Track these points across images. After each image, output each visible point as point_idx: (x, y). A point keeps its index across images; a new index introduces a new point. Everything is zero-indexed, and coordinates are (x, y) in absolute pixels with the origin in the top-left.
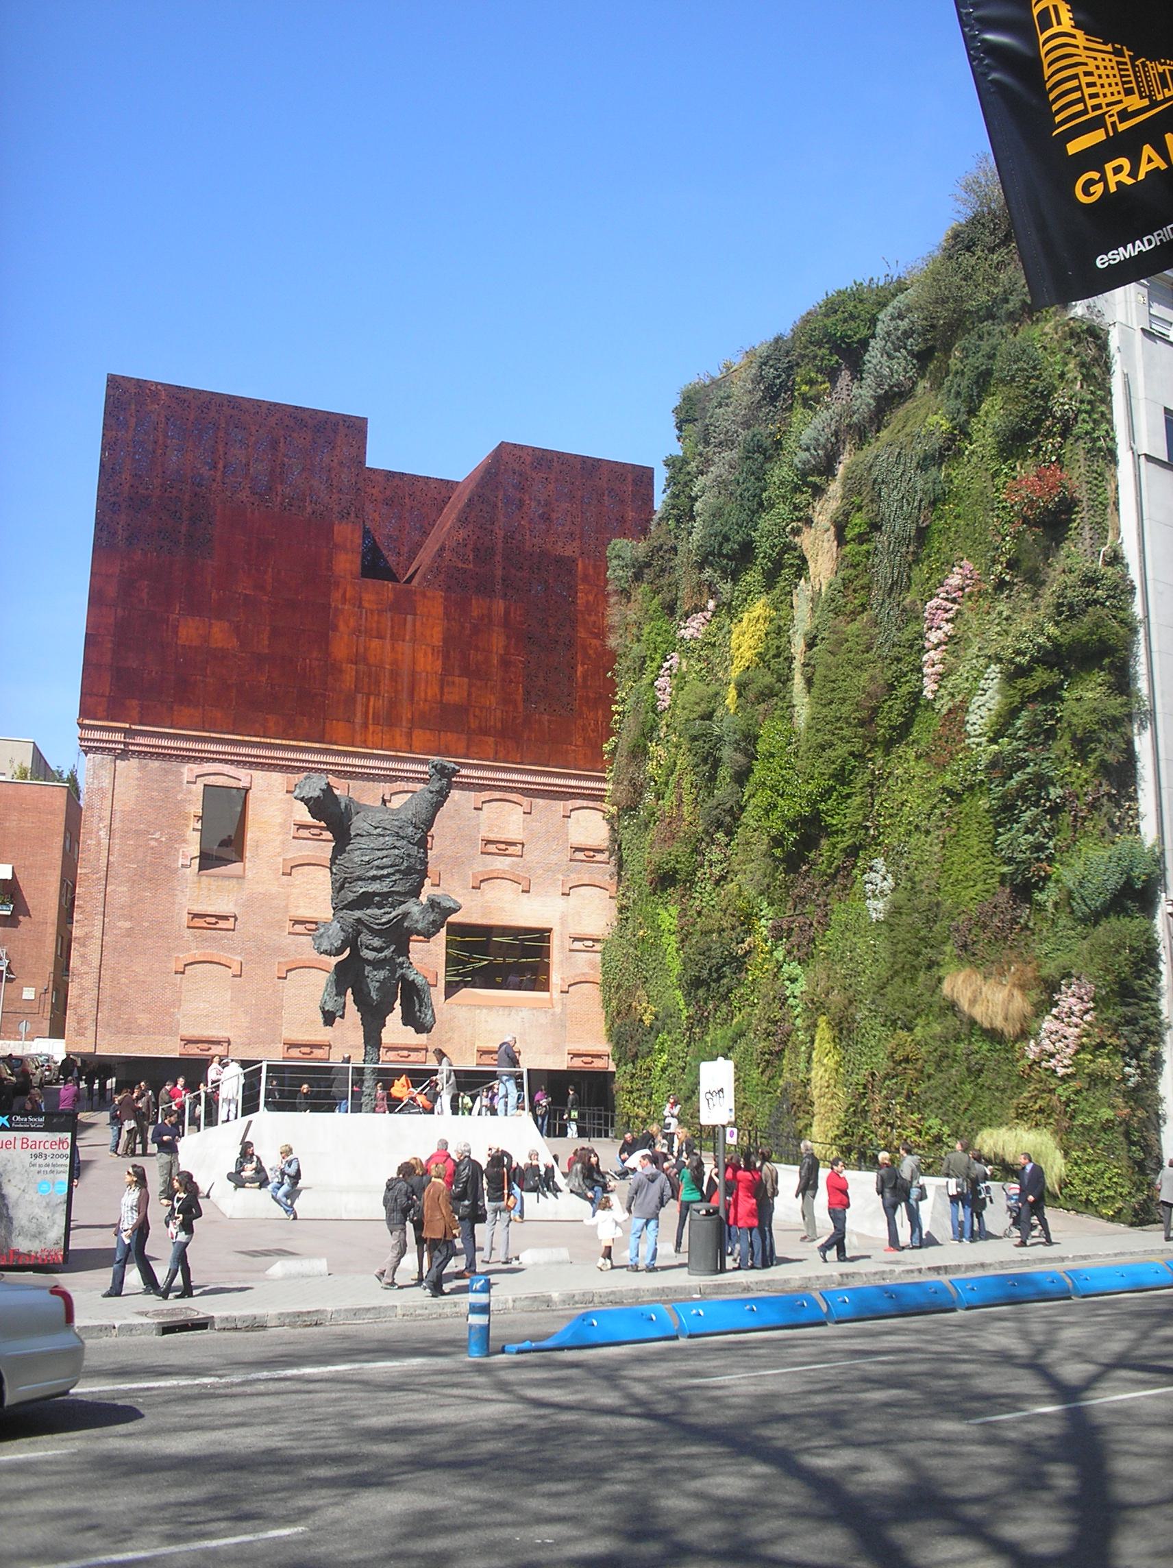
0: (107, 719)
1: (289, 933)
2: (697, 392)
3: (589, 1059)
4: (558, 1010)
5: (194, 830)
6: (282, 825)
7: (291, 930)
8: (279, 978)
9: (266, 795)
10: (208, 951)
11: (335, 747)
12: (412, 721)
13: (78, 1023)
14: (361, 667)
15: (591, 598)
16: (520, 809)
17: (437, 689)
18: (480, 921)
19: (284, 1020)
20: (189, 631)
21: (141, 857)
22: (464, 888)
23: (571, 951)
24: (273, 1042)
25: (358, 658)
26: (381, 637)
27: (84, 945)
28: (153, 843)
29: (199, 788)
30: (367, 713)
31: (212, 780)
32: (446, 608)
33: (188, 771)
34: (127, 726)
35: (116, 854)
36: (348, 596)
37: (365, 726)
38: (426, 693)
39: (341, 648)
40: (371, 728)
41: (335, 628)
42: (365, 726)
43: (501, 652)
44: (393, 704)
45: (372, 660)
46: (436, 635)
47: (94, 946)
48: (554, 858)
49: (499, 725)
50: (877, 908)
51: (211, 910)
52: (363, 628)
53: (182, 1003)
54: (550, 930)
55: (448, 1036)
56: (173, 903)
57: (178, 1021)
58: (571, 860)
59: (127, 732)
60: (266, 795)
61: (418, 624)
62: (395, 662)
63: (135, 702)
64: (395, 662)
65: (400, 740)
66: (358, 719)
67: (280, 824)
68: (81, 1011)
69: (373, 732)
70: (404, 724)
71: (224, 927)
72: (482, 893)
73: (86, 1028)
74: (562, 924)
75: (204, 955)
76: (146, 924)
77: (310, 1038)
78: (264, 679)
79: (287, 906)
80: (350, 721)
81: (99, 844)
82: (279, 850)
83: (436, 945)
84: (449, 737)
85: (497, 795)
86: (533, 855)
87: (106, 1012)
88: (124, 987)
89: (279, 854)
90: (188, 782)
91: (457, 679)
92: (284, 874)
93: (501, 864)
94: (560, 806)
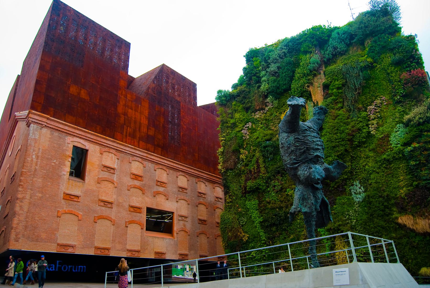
0: (41, 112)
1: (99, 205)
2: (259, 51)
3: (183, 256)
4: (176, 239)
5: (69, 161)
6: (98, 165)
7: (99, 204)
10: (70, 209)
11: (117, 141)
12: (139, 138)
13: (16, 236)
14: (126, 117)
15: (184, 114)
16: (166, 173)
17: (146, 129)
18: (155, 208)
20: (73, 90)
21: (48, 169)
23: (179, 220)
24: (91, 247)
25: (125, 114)
26: (132, 109)
27: (22, 202)
28: (53, 164)
29: (71, 146)
30: (127, 133)
32: (149, 105)
33: (69, 139)
34: (49, 117)
35: (38, 166)
37: (126, 136)
38: (143, 129)
39: (120, 109)
40: (128, 137)
41: (119, 103)
42: (126, 136)
43: (163, 123)
45: (129, 116)
46: (146, 113)
47: (26, 201)
48: (174, 190)
49: (162, 145)
50: (358, 198)
51: (73, 193)
53: (59, 230)
54: (173, 213)
55: (147, 247)
56: (59, 189)
57: (57, 237)
58: (179, 191)
59: (48, 119)
61: (142, 108)
62: (135, 118)
63: (52, 109)
64: (135, 118)
65: (136, 143)
66: (124, 134)
67: (98, 165)
68: (18, 231)
70: (137, 138)
71: (76, 200)
72: (156, 198)
73: (19, 238)
74: (177, 211)
75: (69, 211)
76: (48, 196)
77: (104, 246)
78: (97, 113)
79: (98, 195)
80: (122, 133)
81: (32, 160)
83: (143, 215)
84: (149, 146)
85: (161, 167)
87: (28, 232)
88: (37, 221)
89: (97, 176)
90: (68, 143)
91: (152, 128)
92: (98, 183)
93: (161, 189)
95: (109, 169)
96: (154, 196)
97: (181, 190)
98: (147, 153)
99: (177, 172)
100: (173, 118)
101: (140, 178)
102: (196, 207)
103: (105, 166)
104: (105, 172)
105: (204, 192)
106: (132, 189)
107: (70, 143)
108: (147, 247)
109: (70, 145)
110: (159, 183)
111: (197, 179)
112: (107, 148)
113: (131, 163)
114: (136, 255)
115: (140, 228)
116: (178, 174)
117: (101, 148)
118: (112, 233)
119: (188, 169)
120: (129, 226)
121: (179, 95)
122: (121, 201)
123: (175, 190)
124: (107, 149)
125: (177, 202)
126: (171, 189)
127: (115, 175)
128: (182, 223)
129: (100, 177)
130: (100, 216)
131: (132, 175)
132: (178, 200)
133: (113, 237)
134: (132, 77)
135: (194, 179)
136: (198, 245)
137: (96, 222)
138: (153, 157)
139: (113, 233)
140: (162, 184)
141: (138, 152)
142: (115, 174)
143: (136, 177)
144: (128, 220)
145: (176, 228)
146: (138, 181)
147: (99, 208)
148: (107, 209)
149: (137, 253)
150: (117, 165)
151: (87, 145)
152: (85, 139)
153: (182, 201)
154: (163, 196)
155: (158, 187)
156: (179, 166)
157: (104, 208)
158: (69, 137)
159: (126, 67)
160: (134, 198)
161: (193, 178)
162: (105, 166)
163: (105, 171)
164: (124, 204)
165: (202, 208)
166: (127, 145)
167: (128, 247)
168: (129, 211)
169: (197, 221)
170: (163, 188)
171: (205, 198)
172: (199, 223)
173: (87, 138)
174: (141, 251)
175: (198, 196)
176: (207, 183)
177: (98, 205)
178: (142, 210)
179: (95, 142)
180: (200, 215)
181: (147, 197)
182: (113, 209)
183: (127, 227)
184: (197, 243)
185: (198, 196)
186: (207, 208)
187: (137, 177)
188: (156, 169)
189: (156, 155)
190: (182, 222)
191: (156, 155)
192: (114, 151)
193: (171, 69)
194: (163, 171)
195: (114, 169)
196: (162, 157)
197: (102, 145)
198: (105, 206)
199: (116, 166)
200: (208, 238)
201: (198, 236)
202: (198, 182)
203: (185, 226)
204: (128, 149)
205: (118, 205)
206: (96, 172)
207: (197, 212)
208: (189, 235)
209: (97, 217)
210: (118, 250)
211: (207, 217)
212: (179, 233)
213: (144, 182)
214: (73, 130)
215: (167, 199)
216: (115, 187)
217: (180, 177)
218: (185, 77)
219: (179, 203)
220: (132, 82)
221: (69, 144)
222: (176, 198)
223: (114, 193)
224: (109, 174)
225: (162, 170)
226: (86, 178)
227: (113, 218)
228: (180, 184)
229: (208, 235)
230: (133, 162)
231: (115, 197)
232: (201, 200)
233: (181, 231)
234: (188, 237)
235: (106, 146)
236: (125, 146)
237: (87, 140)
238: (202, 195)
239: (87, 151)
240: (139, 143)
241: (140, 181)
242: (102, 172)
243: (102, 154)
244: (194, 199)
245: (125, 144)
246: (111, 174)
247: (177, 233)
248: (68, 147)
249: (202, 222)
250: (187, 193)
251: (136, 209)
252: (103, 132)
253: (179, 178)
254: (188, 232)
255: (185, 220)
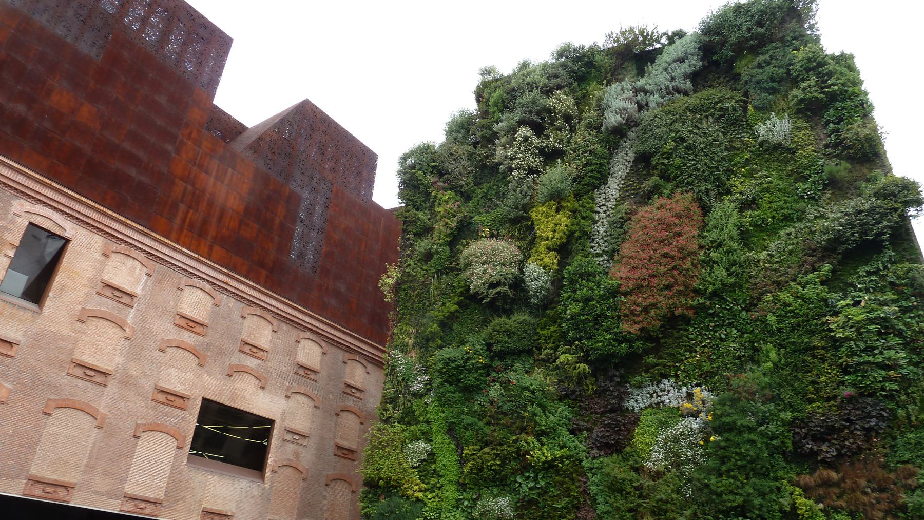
1: (68, 374)
5: (6, 255)
6: (89, 280)
7: (70, 371)
8: (46, 414)
9: (84, 251)
14: (190, 187)
16: (270, 327)
18: (227, 403)
19: (37, 456)
22: (221, 374)
23: (284, 440)
24: (18, 476)
29: (23, 223)
31: (38, 221)
33: (20, 206)
36: (193, 136)
40: (185, 231)
44: (205, 222)
48: (286, 369)
52: (197, 162)
54: (271, 422)
55: (182, 495)
58: (296, 373)
60: (84, 251)
66: (178, 220)
67: (89, 278)
69: (186, 235)
70: (209, 238)
79: (72, 350)
82: (81, 299)
83: (191, 414)
85: (259, 311)
86: (273, 363)
90: (15, 214)
92: (79, 320)
93: (251, 363)
94: (294, 333)
95: (118, 294)
96: (230, 376)
97: (301, 372)
98: (228, 275)
99: (299, 332)
100: (310, 214)
101: (198, 329)
102: (335, 417)
103: (108, 286)
104: (106, 299)
105: (359, 386)
106: (170, 350)
107: (23, 214)
108: (182, 495)
109: (19, 220)
110: (247, 349)
111: (347, 355)
112: (123, 245)
113: (181, 290)
114: (147, 511)
115: (174, 444)
116: (302, 334)
117: (109, 241)
118: (89, 448)
119: (328, 329)
120: (144, 436)
121: (333, 170)
122: (134, 374)
123: (288, 369)
124: (123, 247)
125: (288, 397)
126: (277, 364)
127: (133, 311)
128: (291, 447)
129: (89, 307)
130: (64, 400)
131: (178, 317)
132: (289, 394)
133: (90, 457)
134: (242, 124)
135: (341, 355)
136: (325, 507)
137: (49, 415)
138: (242, 287)
139: (94, 446)
140: (254, 350)
141: (204, 269)
142: (132, 307)
143: (190, 323)
144: (143, 422)
145: (271, 459)
146: (192, 334)
147: (66, 380)
148: (90, 385)
149: (152, 506)
150: (143, 289)
151: (69, 229)
152: (66, 213)
153: (300, 398)
154: (253, 378)
155: (243, 356)
156: (307, 319)
157: (80, 383)
158: (22, 201)
159: (213, 83)
160: (173, 371)
161: (338, 351)
162: (108, 286)
163: (106, 297)
164: (143, 381)
165: (350, 420)
166: (178, 247)
167: (129, 489)
168: (152, 400)
169: (331, 450)
170: (257, 362)
171: (361, 399)
172: (335, 455)
173: (74, 214)
174: (165, 503)
175: (344, 392)
176: (369, 366)
177: (64, 374)
178: (191, 402)
179: (93, 226)
180: (342, 437)
181: (210, 374)
182: (108, 389)
183: (138, 438)
184: (324, 502)
185: (344, 392)
186: (361, 423)
187: (191, 324)
188: (246, 315)
189: (251, 283)
190: (291, 445)
191: (225, 270)
192: (141, 257)
193: (322, 112)
194: (263, 322)
195: (131, 295)
196: (265, 290)
197: (112, 235)
198: (88, 378)
199: (138, 291)
200: (353, 492)
201: (327, 485)
202: (349, 362)
203: (297, 455)
204: (181, 257)
205: (126, 381)
206: (81, 293)
207: (335, 428)
208: (305, 480)
209: (55, 400)
210: (95, 493)
211: (358, 442)
212: (280, 471)
213: (206, 340)
214: (38, 188)
215: (263, 388)
216: (126, 338)
217: (303, 342)
218: (353, 137)
219: (292, 402)
220: (240, 133)
221: (19, 216)
222: (286, 387)
223: (119, 351)
224: (115, 304)
225: (263, 320)
226: (48, 303)
227: (102, 409)
228: (302, 358)
229: (354, 486)
230: (187, 289)
231: (119, 360)
232: (350, 403)
233: (285, 468)
234: (302, 484)
235: (122, 240)
236: (174, 249)
237: (72, 216)
238: (354, 391)
239: (67, 241)
240: (211, 248)
241: (199, 334)
242: (97, 297)
243: (106, 256)
244: (331, 396)
245: (173, 244)
246: (121, 306)
247: (273, 471)
248: (14, 223)
249: (345, 453)
250: (316, 381)
251: (173, 398)
252: (119, 206)
253: (300, 345)
254: (304, 472)
255: (301, 442)
